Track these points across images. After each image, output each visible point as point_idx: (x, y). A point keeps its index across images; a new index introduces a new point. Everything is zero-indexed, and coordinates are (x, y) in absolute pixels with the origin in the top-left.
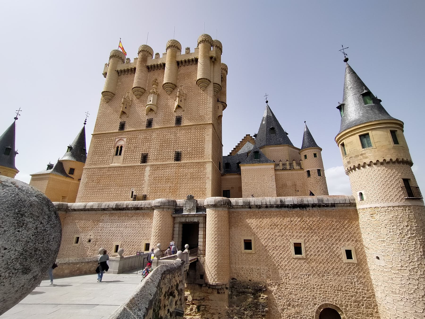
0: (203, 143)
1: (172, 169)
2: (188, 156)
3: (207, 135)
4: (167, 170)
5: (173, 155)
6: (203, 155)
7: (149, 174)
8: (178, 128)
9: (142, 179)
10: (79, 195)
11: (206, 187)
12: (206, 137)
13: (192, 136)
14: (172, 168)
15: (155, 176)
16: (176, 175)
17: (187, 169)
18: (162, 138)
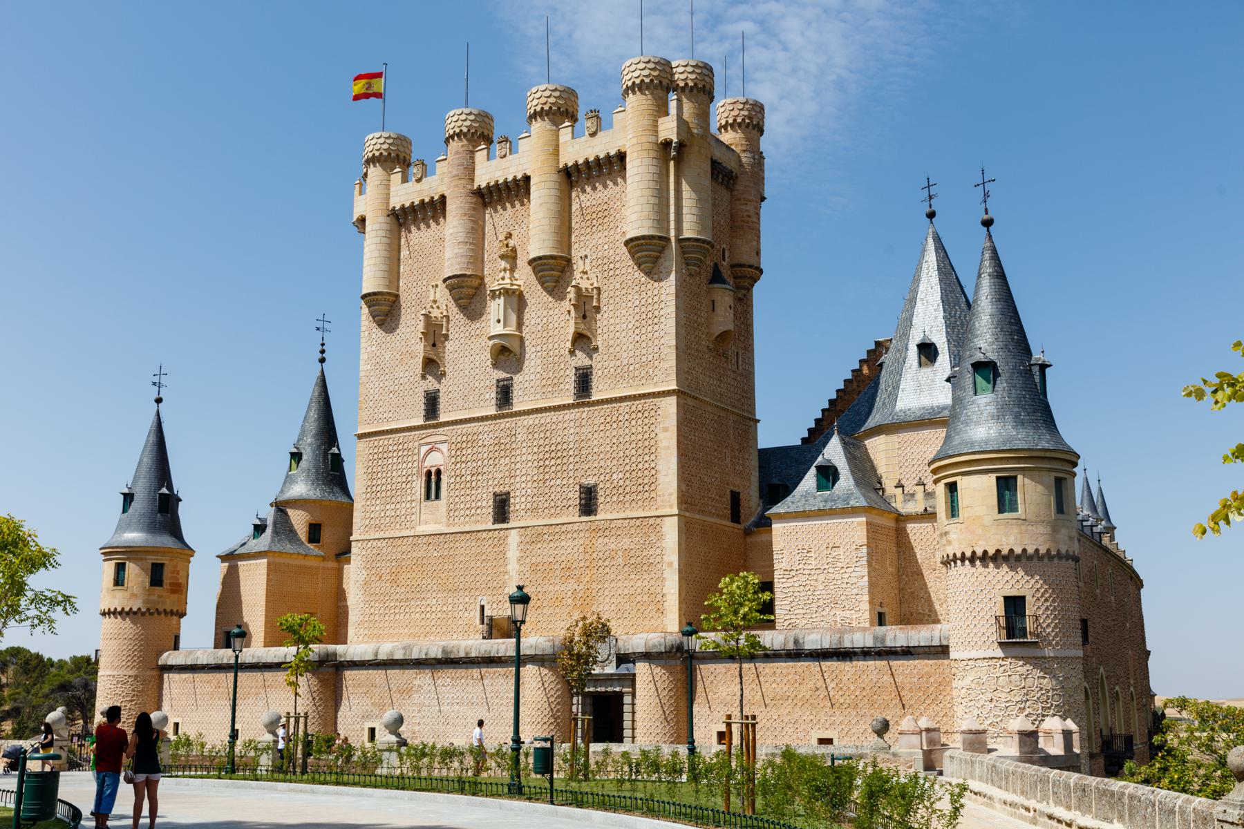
0: (653, 457)
1: (574, 539)
2: (615, 498)
3: (666, 430)
4: (563, 543)
5: (574, 497)
6: (653, 495)
7: (518, 554)
9: (502, 569)
10: (353, 617)
11: (665, 591)
12: (661, 436)
13: (621, 432)
14: (575, 535)
15: (534, 560)
16: (587, 556)
17: (613, 539)
18: (541, 442)
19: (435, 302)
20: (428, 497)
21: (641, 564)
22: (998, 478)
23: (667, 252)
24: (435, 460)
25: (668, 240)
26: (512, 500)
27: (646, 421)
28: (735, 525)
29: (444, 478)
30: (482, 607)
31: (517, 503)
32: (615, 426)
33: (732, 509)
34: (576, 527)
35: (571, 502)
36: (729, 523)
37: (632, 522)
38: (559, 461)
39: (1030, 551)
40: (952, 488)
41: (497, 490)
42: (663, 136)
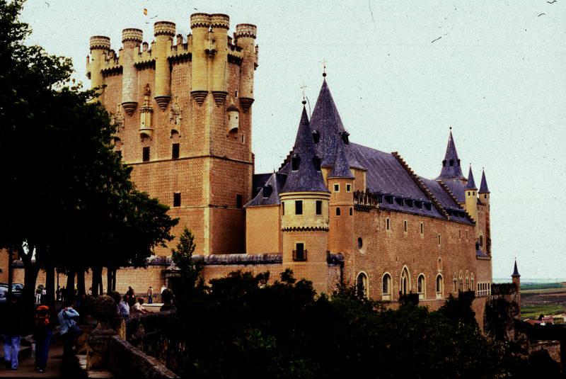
8: (176, 161)
22: (296, 202)
39: (305, 227)
40: (283, 203)
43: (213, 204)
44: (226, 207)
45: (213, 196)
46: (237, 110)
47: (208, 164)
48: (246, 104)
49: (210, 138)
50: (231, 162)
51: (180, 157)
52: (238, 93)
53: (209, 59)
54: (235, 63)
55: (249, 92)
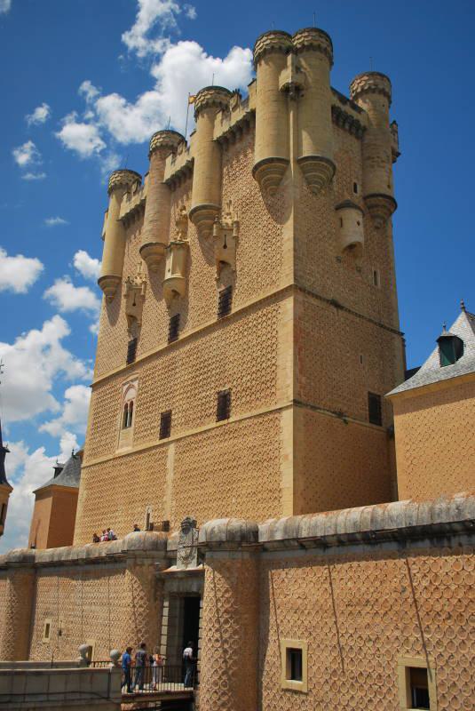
5: (213, 406)
6: (273, 390)
13: (250, 337)
19: (139, 274)
20: (125, 426)
21: (264, 459)
23: (287, 173)
24: (132, 394)
25: (287, 162)
26: (173, 417)
27: (269, 322)
28: (374, 426)
29: (134, 407)
30: (149, 515)
31: (176, 418)
32: (246, 333)
33: (371, 410)
34: (213, 433)
35: (212, 410)
36: (368, 424)
37: (256, 421)
38: (205, 376)
41: (164, 410)
42: (281, 86)
43: (303, 399)
44: (340, 414)
45: (303, 380)
46: (359, 208)
47: (288, 305)
48: (379, 208)
49: (295, 250)
50: (351, 317)
51: (233, 311)
52: (359, 188)
53: (291, 104)
54: (351, 134)
55: (385, 186)
